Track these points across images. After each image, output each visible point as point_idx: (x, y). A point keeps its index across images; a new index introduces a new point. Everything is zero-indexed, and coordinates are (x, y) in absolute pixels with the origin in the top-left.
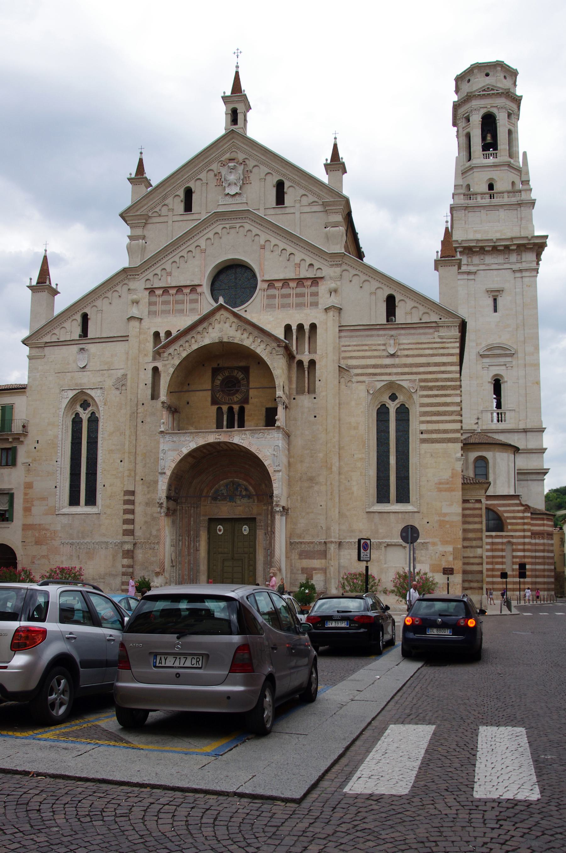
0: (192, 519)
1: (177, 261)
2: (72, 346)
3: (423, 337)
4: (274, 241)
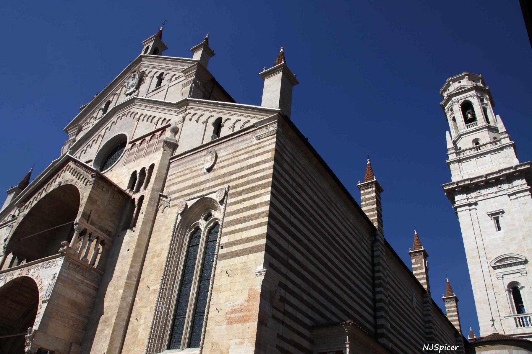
3: (240, 144)
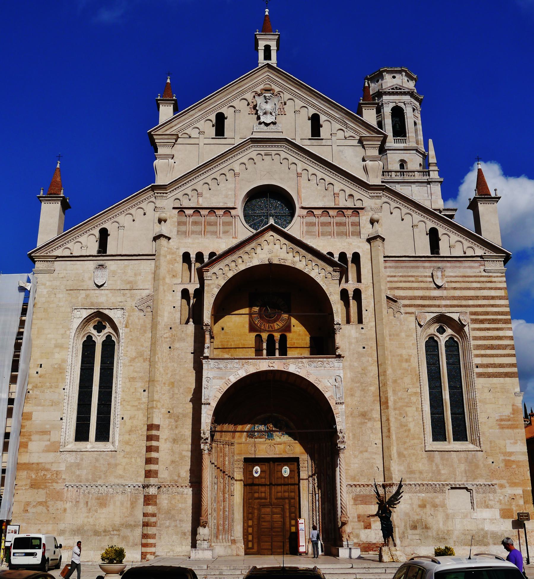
0: (227, 458)
2: (88, 262)
4: (311, 170)
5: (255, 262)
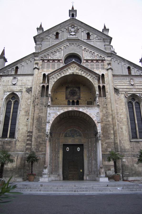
0: (57, 144)
1: (53, 52)
4: (87, 49)
5: (68, 74)
